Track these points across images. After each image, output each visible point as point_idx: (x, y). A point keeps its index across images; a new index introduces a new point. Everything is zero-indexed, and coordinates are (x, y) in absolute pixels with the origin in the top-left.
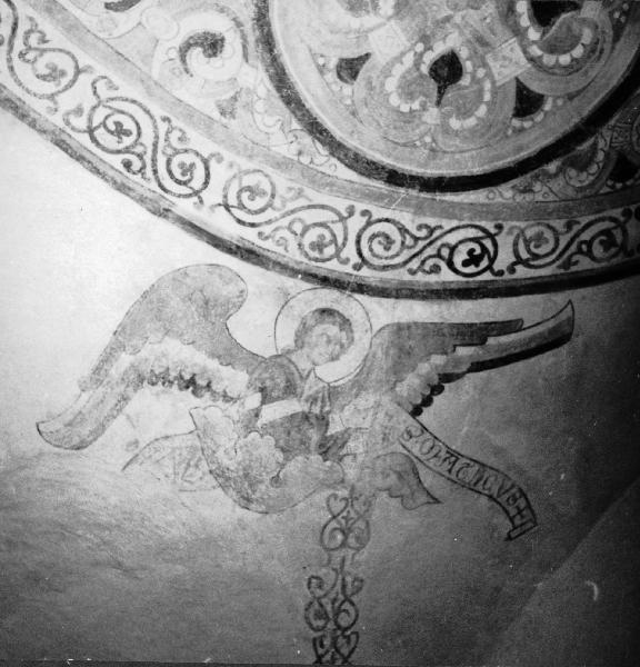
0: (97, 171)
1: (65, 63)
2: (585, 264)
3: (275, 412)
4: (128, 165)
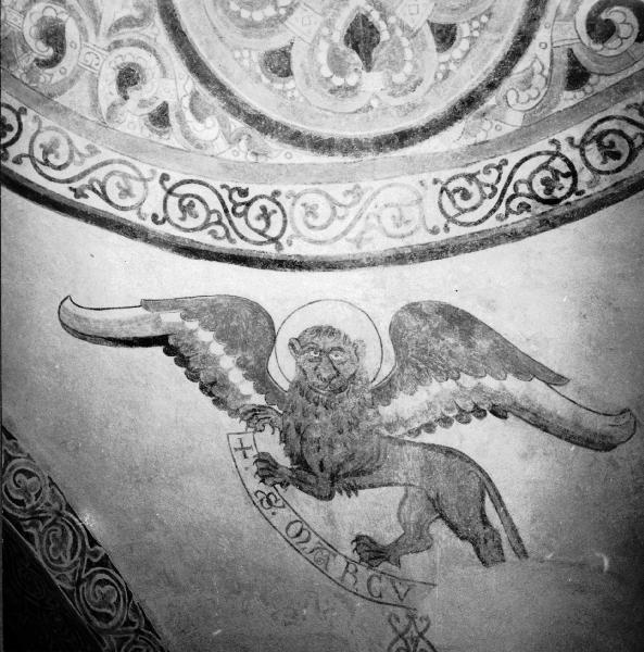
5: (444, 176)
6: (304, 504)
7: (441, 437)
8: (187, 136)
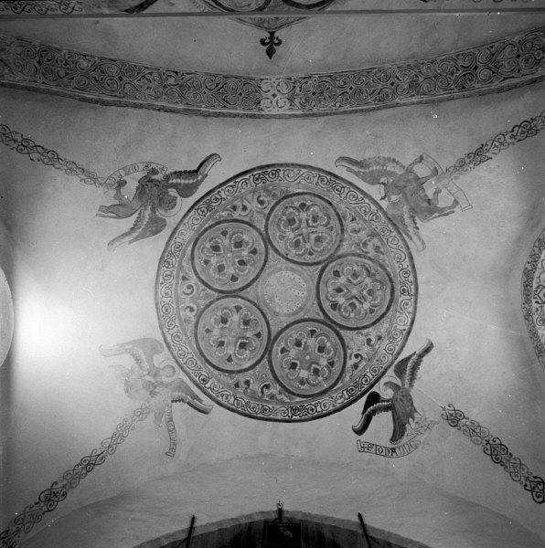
2: (220, 399)
3: (149, 378)
6: (140, 175)
7: (136, 215)
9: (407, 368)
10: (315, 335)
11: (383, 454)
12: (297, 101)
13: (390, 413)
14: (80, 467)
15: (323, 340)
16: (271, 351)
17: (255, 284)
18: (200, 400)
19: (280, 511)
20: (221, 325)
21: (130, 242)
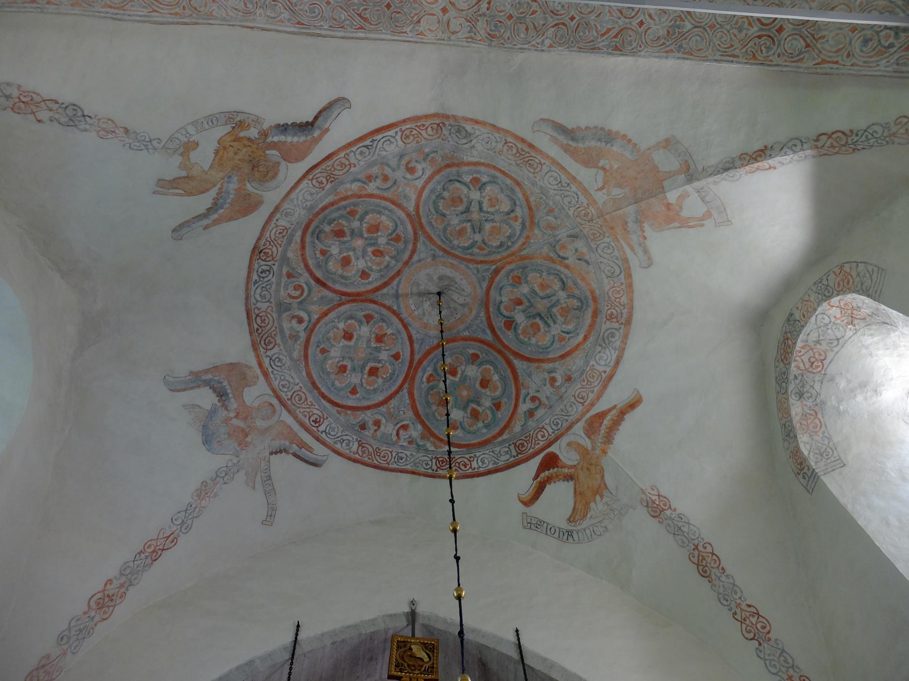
0: (249, 325)
1: (268, 297)
2: (338, 446)
3: (236, 422)
4: (257, 330)
5: (289, 231)
8: (359, 180)
9: (604, 426)
10: (479, 361)
11: (556, 535)
12: (481, 25)
13: (571, 484)
14: (143, 556)
15: (488, 371)
16: (413, 378)
17: (395, 283)
18: (310, 449)
19: (412, 616)
20: (344, 342)
21: (206, 228)
